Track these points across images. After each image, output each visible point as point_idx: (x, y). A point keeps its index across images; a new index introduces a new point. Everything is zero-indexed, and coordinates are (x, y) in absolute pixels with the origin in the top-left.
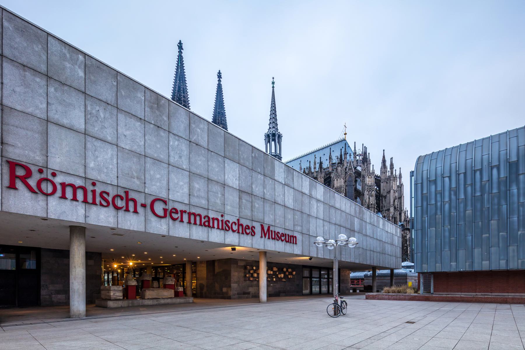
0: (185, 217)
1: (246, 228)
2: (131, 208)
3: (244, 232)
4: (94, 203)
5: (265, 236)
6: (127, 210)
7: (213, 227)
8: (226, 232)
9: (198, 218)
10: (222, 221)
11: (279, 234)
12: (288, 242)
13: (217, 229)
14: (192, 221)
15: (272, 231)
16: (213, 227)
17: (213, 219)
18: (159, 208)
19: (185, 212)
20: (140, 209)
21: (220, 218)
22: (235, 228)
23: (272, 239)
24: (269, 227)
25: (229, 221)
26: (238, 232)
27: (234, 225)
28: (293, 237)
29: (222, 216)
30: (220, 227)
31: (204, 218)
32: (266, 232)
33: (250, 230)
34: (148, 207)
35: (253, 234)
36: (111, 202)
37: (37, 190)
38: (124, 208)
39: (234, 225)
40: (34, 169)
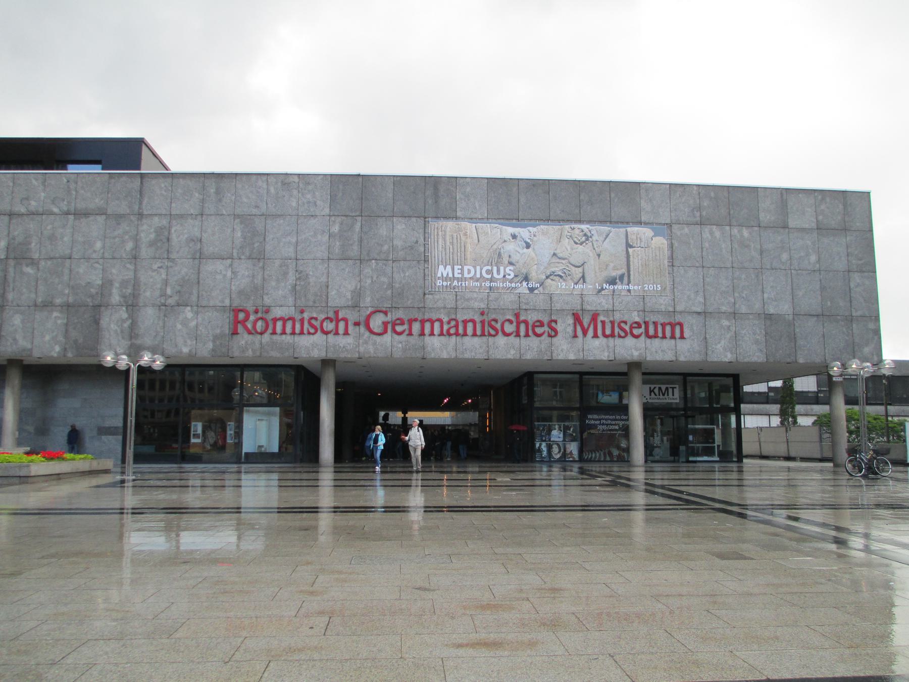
0: (416, 327)
1: (534, 326)
3: (530, 333)
4: (302, 333)
5: (585, 332)
6: (337, 333)
7: (465, 334)
8: (491, 339)
9: (437, 325)
10: (483, 322)
12: (656, 336)
15: (603, 322)
16: (465, 334)
17: (465, 322)
18: (377, 322)
19: (416, 320)
20: (351, 328)
21: (478, 318)
22: (509, 328)
23: (605, 336)
24: (594, 318)
25: (496, 321)
26: (518, 335)
27: (507, 325)
28: (673, 326)
29: (482, 314)
30: (479, 332)
31: (449, 323)
32: (586, 325)
33: (546, 328)
35: (553, 334)
36: (318, 327)
37: (253, 332)
39: (507, 325)
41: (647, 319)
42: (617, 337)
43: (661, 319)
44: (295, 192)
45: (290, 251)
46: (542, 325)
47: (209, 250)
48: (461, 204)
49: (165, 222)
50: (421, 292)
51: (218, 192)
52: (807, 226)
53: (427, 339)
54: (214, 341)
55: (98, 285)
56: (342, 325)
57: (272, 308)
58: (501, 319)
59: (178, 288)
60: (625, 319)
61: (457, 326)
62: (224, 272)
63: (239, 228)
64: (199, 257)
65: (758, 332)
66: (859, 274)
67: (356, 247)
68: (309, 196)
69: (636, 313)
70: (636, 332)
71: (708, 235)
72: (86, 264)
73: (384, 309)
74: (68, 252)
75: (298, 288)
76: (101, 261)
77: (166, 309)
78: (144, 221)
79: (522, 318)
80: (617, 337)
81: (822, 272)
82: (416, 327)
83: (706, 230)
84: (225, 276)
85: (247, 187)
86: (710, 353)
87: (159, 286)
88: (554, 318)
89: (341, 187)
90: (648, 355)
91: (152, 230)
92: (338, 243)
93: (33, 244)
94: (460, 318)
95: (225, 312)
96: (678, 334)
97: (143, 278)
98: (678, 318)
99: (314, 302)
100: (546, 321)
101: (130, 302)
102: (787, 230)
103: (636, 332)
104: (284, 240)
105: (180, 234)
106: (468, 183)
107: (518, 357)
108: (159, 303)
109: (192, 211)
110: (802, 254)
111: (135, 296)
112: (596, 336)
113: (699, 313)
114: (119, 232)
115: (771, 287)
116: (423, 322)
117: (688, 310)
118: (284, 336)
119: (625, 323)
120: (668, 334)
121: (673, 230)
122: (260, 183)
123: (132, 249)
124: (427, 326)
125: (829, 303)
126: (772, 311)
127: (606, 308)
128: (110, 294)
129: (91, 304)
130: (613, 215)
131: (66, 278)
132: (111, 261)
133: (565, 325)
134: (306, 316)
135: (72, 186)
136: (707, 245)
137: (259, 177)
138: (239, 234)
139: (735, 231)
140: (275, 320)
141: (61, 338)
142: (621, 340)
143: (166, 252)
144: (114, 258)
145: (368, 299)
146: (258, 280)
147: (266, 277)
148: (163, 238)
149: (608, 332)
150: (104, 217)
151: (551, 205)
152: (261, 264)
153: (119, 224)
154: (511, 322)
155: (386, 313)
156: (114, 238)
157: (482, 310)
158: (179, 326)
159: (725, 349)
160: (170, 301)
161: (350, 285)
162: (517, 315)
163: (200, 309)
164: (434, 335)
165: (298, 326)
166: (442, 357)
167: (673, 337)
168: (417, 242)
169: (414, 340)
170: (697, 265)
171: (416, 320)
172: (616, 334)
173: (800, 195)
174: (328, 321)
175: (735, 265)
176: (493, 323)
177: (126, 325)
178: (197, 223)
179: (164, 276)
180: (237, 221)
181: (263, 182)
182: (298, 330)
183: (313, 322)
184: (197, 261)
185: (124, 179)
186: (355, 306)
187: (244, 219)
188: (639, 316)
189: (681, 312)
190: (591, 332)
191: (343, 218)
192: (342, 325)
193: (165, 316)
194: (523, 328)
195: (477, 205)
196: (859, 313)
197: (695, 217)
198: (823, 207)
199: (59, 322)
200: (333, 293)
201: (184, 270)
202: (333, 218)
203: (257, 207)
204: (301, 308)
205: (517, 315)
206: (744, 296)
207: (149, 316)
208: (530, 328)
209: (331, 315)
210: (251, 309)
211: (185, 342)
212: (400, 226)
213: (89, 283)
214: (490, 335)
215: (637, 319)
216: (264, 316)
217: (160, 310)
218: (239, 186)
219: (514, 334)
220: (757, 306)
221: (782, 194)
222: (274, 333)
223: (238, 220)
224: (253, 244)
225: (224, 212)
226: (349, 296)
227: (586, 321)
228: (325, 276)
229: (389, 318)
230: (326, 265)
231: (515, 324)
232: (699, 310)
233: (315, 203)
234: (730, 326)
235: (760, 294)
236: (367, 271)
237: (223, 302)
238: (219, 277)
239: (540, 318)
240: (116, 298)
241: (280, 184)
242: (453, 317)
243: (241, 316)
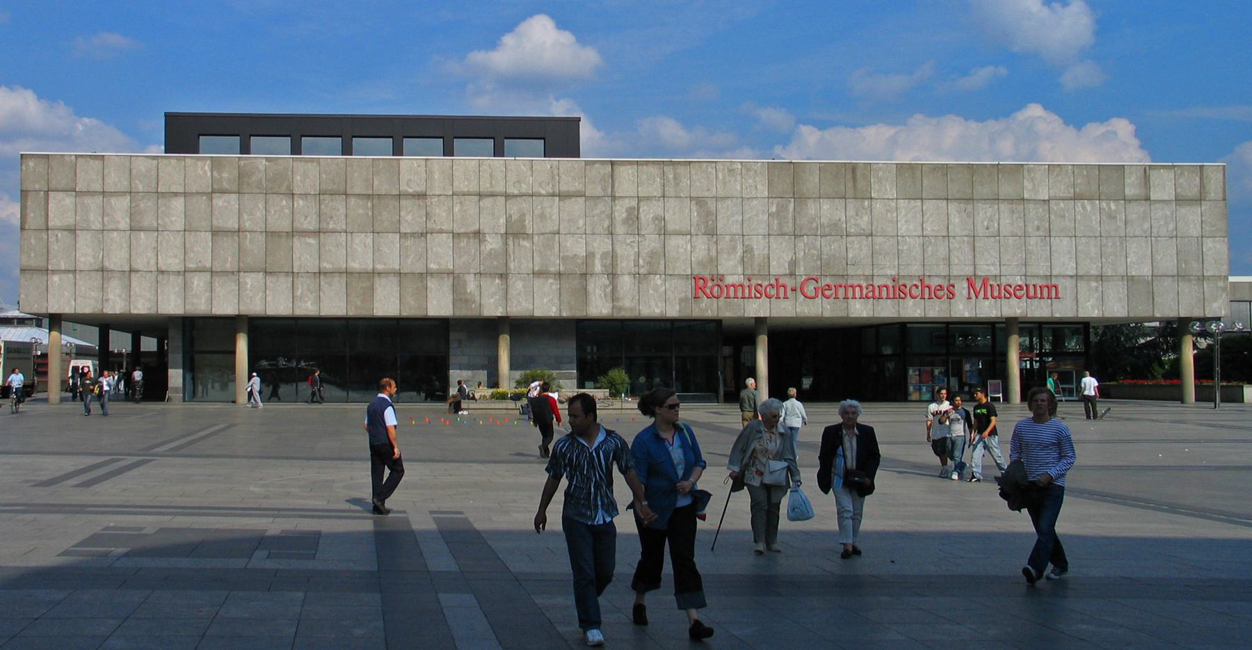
0: (841, 292)
2: (782, 295)
4: (750, 297)
7: (880, 298)
8: (900, 300)
9: (858, 289)
12: (1035, 297)
14: (850, 295)
18: (810, 288)
21: (890, 283)
22: (916, 292)
24: (984, 284)
26: (923, 298)
27: (914, 288)
32: (978, 289)
34: (798, 290)
41: (1028, 283)
43: (1040, 282)
44: (739, 177)
45: (736, 229)
47: (670, 227)
48: (875, 187)
49: (634, 203)
50: (844, 262)
51: (675, 178)
52: (1166, 198)
54: (680, 304)
55: (583, 256)
58: (909, 285)
59: (648, 259)
60: (1009, 283)
61: (873, 291)
62: (685, 247)
63: (694, 208)
64: (664, 232)
65: (1121, 291)
66: (1211, 239)
67: (791, 225)
68: (750, 181)
69: (1019, 277)
70: (1018, 293)
71: (1080, 208)
72: (572, 238)
73: (815, 277)
74: (556, 228)
75: (745, 259)
76: (584, 236)
77: (640, 278)
78: (617, 202)
79: (927, 282)
81: (1178, 239)
82: (841, 292)
83: (1079, 203)
84: (686, 249)
85: (699, 173)
86: (1080, 310)
87: (632, 258)
88: (952, 282)
89: (776, 173)
90: (1029, 313)
91: (624, 210)
92: (776, 222)
93: (527, 222)
94: (877, 282)
96: (1053, 295)
97: (619, 251)
98: (1054, 282)
99: (759, 271)
100: (945, 284)
101: (610, 271)
102: (1149, 202)
103: (1018, 293)
104: (732, 219)
105: (648, 213)
106: (880, 169)
108: (633, 272)
109: (655, 194)
110: (1162, 223)
111: (613, 264)
112: (986, 298)
113: (1071, 276)
114: (597, 211)
115: (1134, 252)
117: (1062, 274)
120: (1045, 294)
121: (1051, 206)
122: (710, 169)
123: (609, 227)
124: (850, 290)
125: (1184, 266)
126: (1134, 273)
127: (994, 274)
128: (593, 265)
129: (579, 272)
130: (1000, 193)
131: (557, 250)
132: (591, 236)
133: (961, 288)
134: (754, 282)
135: (556, 172)
136: (1079, 217)
137: (709, 164)
138: (696, 214)
139: (1104, 204)
141: (556, 301)
142: (1007, 300)
143: (636, 230)
144: (593, 234)
145: (802, 268)
146: (713, 253)
147: (719, 250)
148: (633, 217)
149: (996, 294)
150: (584, 198)
151: (949, 187)
152: (715, 239)
153: (596, 205)
156: (593, 217)
158: (651, 292)
159: (1093, 307)
160: (642, 271)
161: (787, 257)
163: (668, 277)
164: (856, 298)
165: (747, 291)
166: (862, 316)
167: (1049, 297)
168: (840, 220)
169: (841, 303)
170: (1070, 235)
172: (1003, 295)
173: (1162, 171)
175: (1103, 235)
177: (609, 290)
178: (661, 203)
179: (637, 250)
180: (693, 202)
181: (712, 168)
182: (747, 295)
184: (662, 237)
185: (597, 165)
186: (792, 274)
187: (699, 201)
189: (1056, 276)
191: (779, 199)
193: (639, 283)
195: (888, 189)
196: (1209, 274)
197: (1069, 193)
198: (1181, 180)
199: (554, 287)
200: (773, 263)
201: (653, 245)
202: (771, 200)
203: (708, 190)
206: (1110, 261)
207: (626, 283)
208: (933, 289)
209: (773, 281)
210: (709, 277)
211: (657, 304)
212: (826, 206)
213: (576, 255)
215: (1020, 283)
216: (720, 283)
217: (634, 277)
218: (693, 172)
220: (1121, 270)
221: (1145, 170)
223: (694, 202)
224: (708, 222)
225: (682, 195)
226: (787, 265)
227: (978, 285)
228: (767, 249)
230: (767, 240)
231: (920, 288)
232: (1071, 274)
233: (756, 187)
234: (1097, 287)
235: (1123, 259)
236: (801, 245)
237: (685, 271)
238: (681, 250)
239: (940, 283)
240: (598, 267)
241: (726, 170)
242: (871, 283)
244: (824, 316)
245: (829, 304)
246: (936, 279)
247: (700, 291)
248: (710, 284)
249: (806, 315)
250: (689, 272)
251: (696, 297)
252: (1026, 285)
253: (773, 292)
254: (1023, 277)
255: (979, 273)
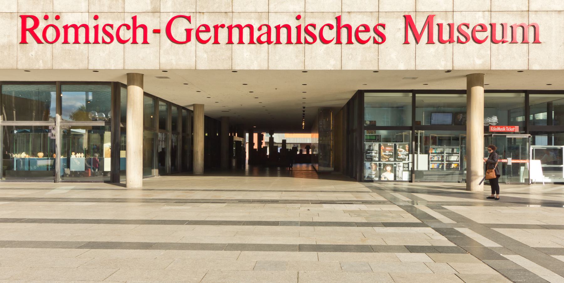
0: (223, 34)
1: (357, 31)
3: (353, 39)
4: (96, 42)
5: (417, 39)
6: (135, 42)
9: (246, 31)
10: (299, 28)
11: (468, 27)
13: (296, 43)
14: (236, 38)
16: (278, 42)
17: (278, 28)
18: (179, 32)
19: (223, 26)
20: (150, 35)
21: (294, 24)
23: (441, 41)
24: (429, 21)
25: (314, 26)
27: (326, 29)
31: (260, 29)
32: (419, 31)
33: (372, 34)
34: (163, 32)
35: (380, 40)
37: (43, 41)
38: (131, 41)
39: (326, 29)
40: (40, 17)
41: (493, 22)
42: (455, 43)
43: (510, 20)
46: (367, 29)
53: (236, 46)
56: (140, 32)
57: (63, 14)
60: (466, 22)
70: (480, 36)
73: (187, 15)
80: (455, 43)
82: (223, 34)
95: (12, 18)
96: (531, 37)
98: (533, 19)
99: (110, 7)
107: (338, 68)
116: (230, 28)
118: (77, 45)
119: (467, 26)
120: (519, 38)
124: (235, 32)
127: (443, 9)
134: (101, 23)
140: (66, 28)
149: (446, 37)
154: (331, 27)
155: (189, 19)
157: (298, 14)
162: (338, 19)
164: (243, 43)
167: (524, 41)
171: (223, 26)
172: (455, 39)
174: (125, 27)
176: (310, 28)
182: (92, 38)
183: (108, 29)
186: (156, 12)
188: (484, 17)
190: (424, 38)
192: (140, 32)
194: (344, 32)
204: (95, 14)
205: (338, 19)
214: (306, 42)
215: (482, 22)
216: (56, 23)
219: (335, 41)
222: (66, 42)
227: (419, 24)
229: (194, 26)
231: (335, 29)
243: (30, 23)
244: (197, 68)
245: (206, 52)
246: (360, 16)
247: (28, 33)
248: (43, 24)
249: (174, 68)
250: (14, 9)
251: (24, 41)
252: (491, 25)
253: (126, 34)
254: (487, 14)
255: (420, 8)
